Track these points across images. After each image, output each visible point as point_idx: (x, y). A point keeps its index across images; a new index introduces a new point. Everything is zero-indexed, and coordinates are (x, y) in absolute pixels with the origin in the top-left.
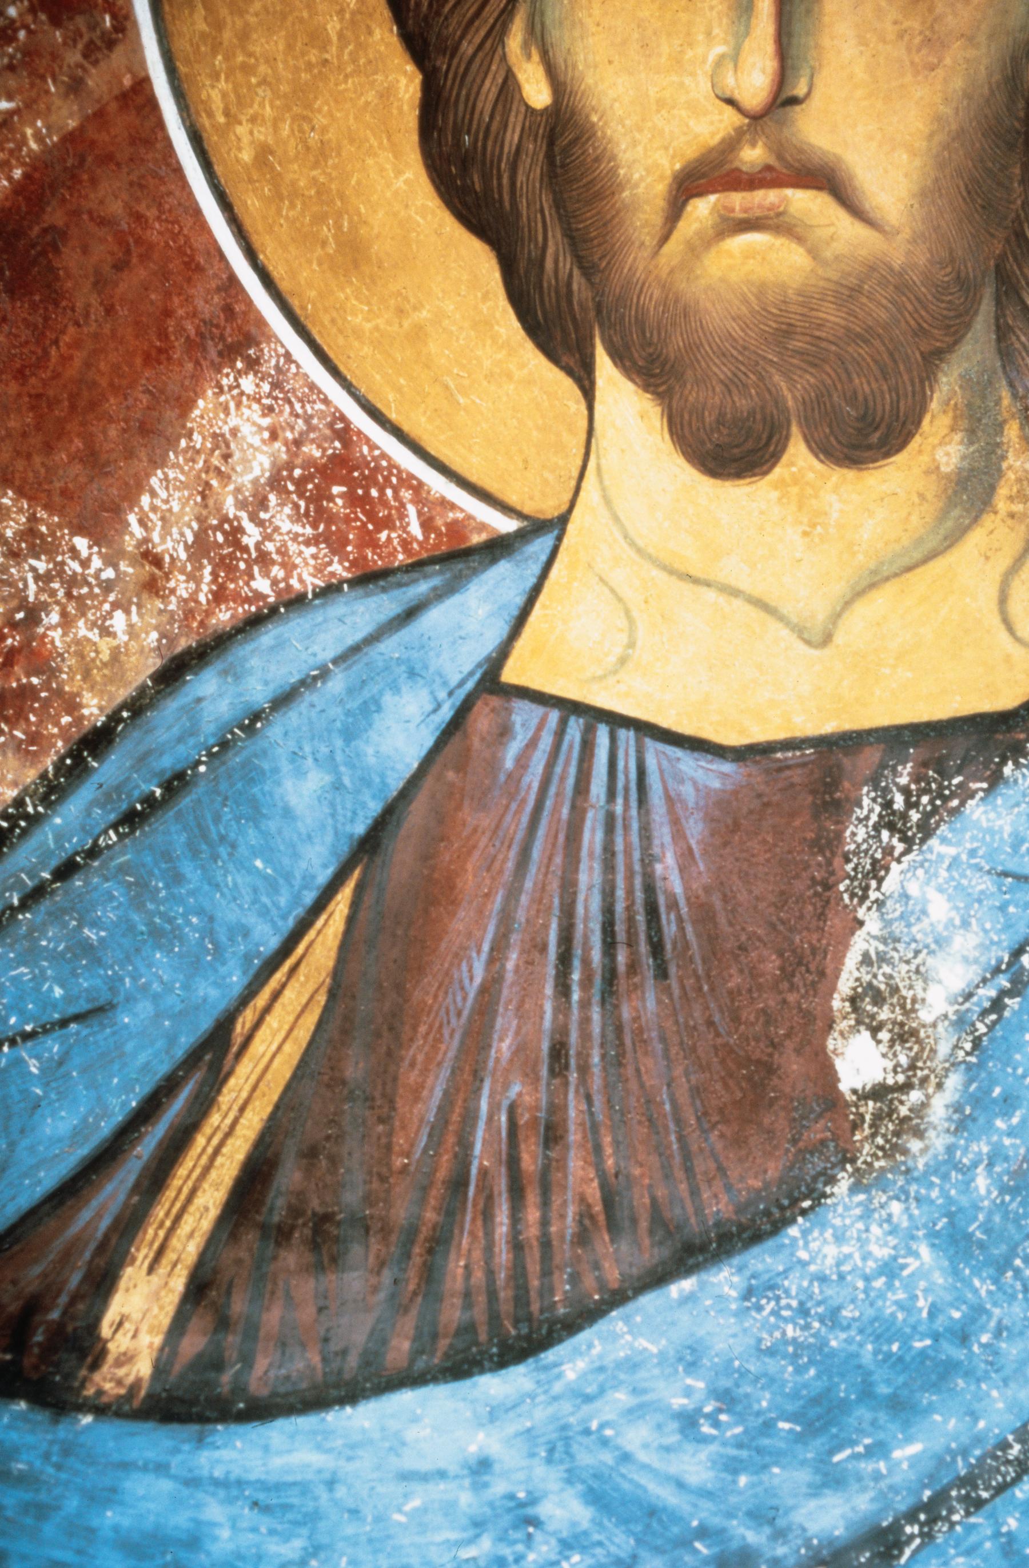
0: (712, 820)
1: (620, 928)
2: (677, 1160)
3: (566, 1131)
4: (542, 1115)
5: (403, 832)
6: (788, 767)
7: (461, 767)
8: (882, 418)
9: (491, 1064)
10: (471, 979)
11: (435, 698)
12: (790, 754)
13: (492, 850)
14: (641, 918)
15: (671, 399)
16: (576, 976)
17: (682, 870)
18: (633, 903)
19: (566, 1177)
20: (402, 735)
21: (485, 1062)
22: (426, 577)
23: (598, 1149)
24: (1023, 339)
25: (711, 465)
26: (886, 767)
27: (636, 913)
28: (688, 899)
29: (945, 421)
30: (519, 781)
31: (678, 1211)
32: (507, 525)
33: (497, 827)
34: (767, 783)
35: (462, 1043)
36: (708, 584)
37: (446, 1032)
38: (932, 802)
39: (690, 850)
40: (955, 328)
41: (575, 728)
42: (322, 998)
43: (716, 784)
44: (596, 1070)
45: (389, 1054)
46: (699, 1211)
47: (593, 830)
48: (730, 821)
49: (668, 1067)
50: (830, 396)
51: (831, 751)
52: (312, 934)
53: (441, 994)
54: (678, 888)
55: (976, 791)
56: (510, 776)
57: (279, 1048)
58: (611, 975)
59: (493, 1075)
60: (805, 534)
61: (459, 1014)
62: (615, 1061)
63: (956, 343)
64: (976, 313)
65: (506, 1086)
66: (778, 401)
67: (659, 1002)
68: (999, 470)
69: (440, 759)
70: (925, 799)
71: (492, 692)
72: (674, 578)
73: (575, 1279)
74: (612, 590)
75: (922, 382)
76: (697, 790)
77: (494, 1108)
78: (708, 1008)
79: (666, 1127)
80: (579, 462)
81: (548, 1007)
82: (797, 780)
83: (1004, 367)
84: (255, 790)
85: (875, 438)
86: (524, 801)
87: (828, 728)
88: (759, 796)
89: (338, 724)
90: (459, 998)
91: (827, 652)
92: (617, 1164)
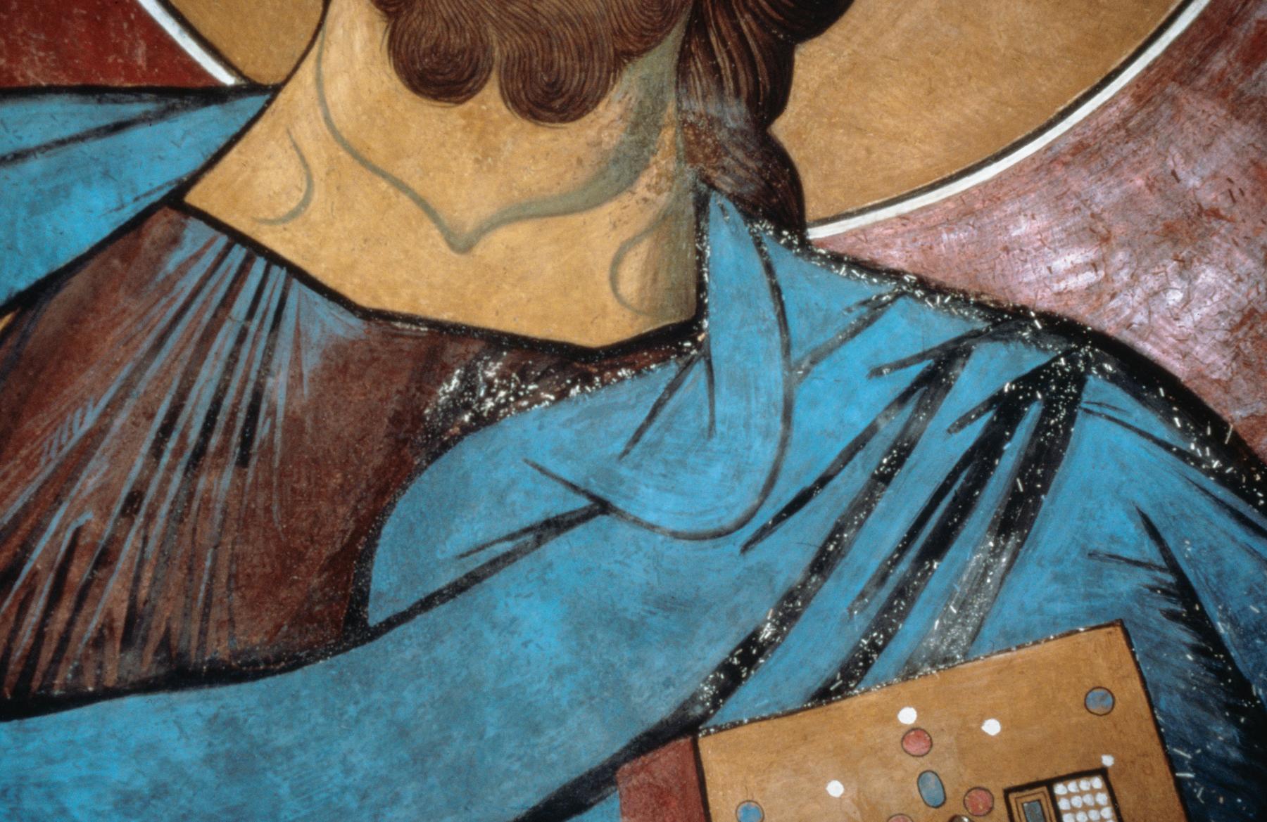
0: (327, 358)
1: (222, 419)
2: (200, 604)
3: (116, 559)
4: (102, 542)
5: (60, 296)
6: (402, 336)
7: (126, 258)
8: (568, 91)
9: (74, 492)
10: (81, 424)
12: (407, 327)
13: (134, 331)
14: (242, 415)
15: (397, 18)
16: (171, 444)
17: (290, 389)
18: (240, 402)
19: (102, 593)
20: (85, 219)
21: (69, 490)
22: (141, 101)
23: (137, 579)
24: (699, 65)
25: (416, 83)
26: (480, 359)
27: (239, 410)
29: (617, 109)
30: (175, 283)
31: (183, 644)
32: (227, 79)
33: (145, 313)
34: (382, 344)
35: (55, 471)
36: (384, 175)
37: (43, 460)
38: (507, 397)
39: (301, 375)
40: (647, 41)
41: (239, 253)
43: (340, 332)
44: (161, 520)
46: (202, 645)
47: (226, 337)
48: (341, 362)
49: (220, 534)
50: (531, 59)
51: (440, 334)
55: (544, 400)
56: (168, 277)
58: (200, 452)
59: (72, 502)
60: (477, 161)
61: (60, 448)
62: (177, 517)
63: (646, 50)
64: (668, 32)
65: (80, 512)
66: (486, 48)
67: (233, 482)
68: (647, 160)
69: (110, 249)
70: (502, 393)
72: (356, 162)
73: (78, 672)
74: (302, 158)
75: (609, 72)
76: (323, 331)
78: (270, 498)
79: (200, 578)
80: (304, 46)
81: (139, 462)
82: (406, 348)
83: (677, 83)
85: (557, 104)
86: (174, 299)
87: (446, 316)
88: (371, 351)
90: (65, 437)
91: (463, 258)
92: (149, 594)
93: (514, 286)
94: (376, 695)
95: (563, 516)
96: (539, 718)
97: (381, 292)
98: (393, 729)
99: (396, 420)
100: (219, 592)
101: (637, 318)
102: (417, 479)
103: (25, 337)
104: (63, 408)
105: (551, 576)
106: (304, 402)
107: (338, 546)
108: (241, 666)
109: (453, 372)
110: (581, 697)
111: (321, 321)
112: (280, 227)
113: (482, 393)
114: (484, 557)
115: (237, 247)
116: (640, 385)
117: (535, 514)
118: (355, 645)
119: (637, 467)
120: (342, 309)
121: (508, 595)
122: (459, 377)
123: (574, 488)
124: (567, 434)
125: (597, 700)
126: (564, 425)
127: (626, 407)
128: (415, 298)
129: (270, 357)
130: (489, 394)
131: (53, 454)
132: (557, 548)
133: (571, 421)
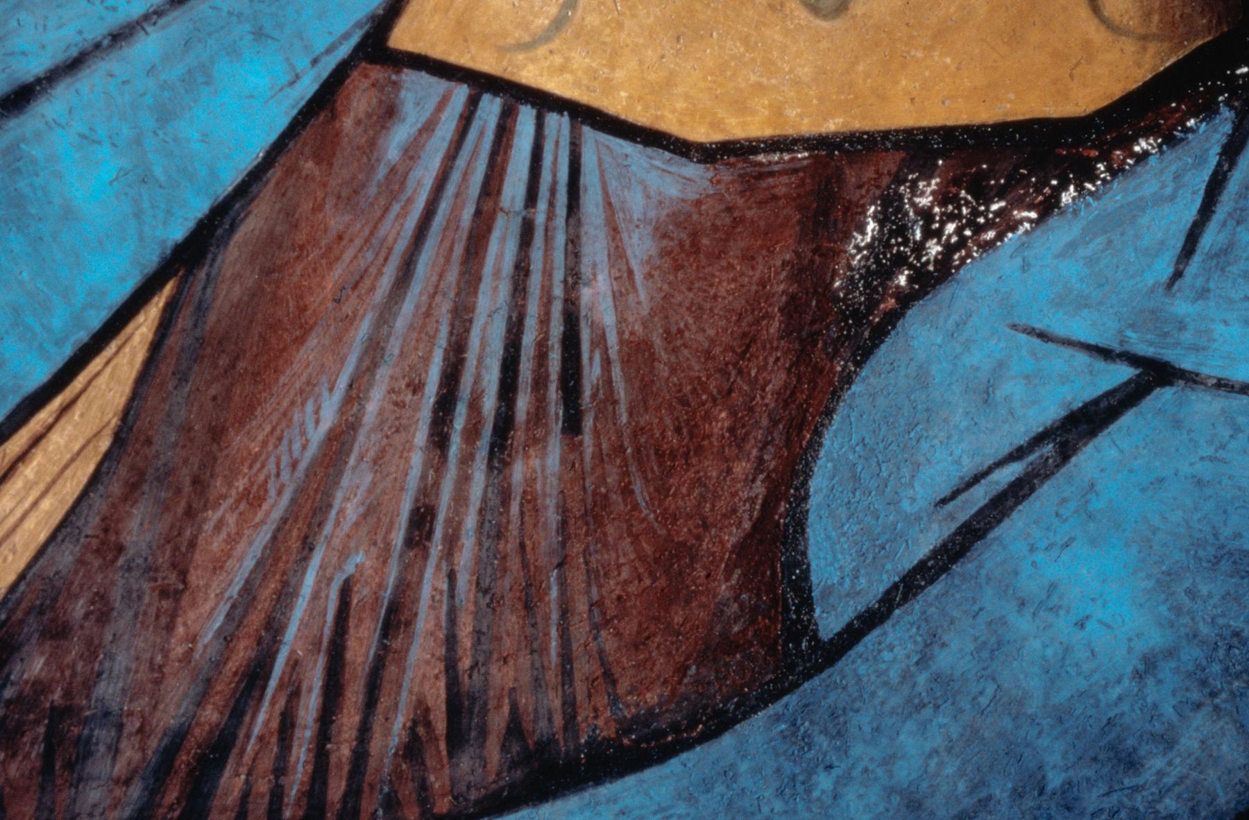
4: (387, 594)
10: (317, 422)
11: (292, 67)
13: (363, 264)
16: (459, 423)
17: (617, 297)
18: (546, 339)
19: (403, 671)
26: (905, 181)
28: (620, 333)
34: (742, 193)
35: (293, 501)
38: (959, 232)
39: (630, 273)
41: (491, 107)
42: (105, 444)
43: (673, 191)
44: (468, 542)
45: (190, 513)
47: (503, 239)
49: (563, 544)
51: (831, 155)
52: (96, 364)
53: (272, 441)
54: (608, 319)
55: (1021, 222)
57: (35, 504)
58: (504, 423)
59: (329, 541)
61: (294, 465)
65: (344, 554)
67: (563, 461)
70: (951, 227)
71: (373, 60)
76: (648, 197)
77: (324, 580)
78: (626, 474)
79: (547, 618)
82: (781, 191)
84: (22, 185)
86: (410, 201)
87: (832, 125)
88: (729, 209)
89: (149, 100)
90: (297, 446)
91: (838, 24)
93: (928, 49)
94: (858, 749)
95: (1096, 402)
96: (1130, 742)
97: (721, 113)
98: (896, 799)
99: (793, 307)
100: (580, 630)
101: (1145, 49)
102: (846, 395)
103: (201, 310)
104: (285, 404)
105: (1097, 504)
106: (645, 311)
107: (747, 525)
108: (637, 742)
109: (864, 212)
110: (1195, 696)
111: (641, 182)
112: (542, 51)
113: (918, 236)
114: (980, 495)
115: (486, 98)
116: (1175, 159)
117: (1049, 411)
118: (808, 676)
119: (1203, 294)
120: (667, 155)
121: (1033, 549)
122: (875, 217)
123: (1105, 353)
124: (1072, 269)
125: (1224, 696)
126: (1061, 255)
127: (1159, 200)
128: (778, 111)
129: (577, 255)
130: (928, 234)
131: (285, 476)
132: (1097, 457)
133: (1072, 246)
